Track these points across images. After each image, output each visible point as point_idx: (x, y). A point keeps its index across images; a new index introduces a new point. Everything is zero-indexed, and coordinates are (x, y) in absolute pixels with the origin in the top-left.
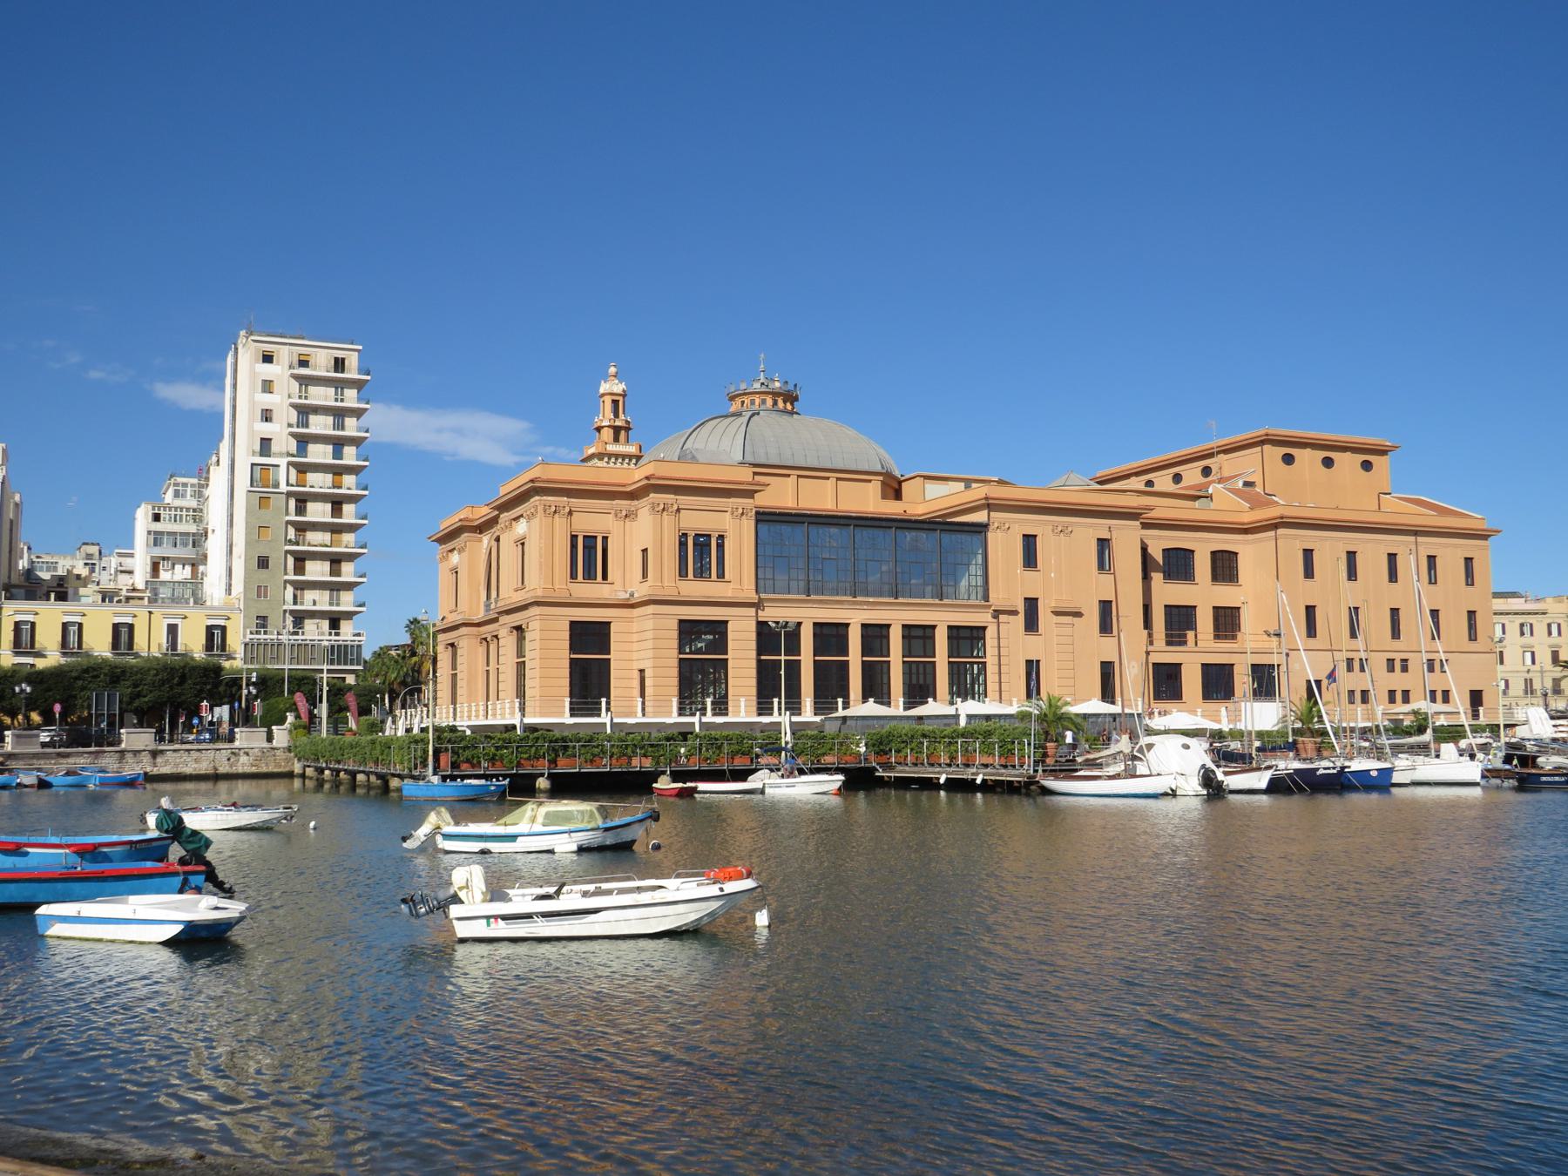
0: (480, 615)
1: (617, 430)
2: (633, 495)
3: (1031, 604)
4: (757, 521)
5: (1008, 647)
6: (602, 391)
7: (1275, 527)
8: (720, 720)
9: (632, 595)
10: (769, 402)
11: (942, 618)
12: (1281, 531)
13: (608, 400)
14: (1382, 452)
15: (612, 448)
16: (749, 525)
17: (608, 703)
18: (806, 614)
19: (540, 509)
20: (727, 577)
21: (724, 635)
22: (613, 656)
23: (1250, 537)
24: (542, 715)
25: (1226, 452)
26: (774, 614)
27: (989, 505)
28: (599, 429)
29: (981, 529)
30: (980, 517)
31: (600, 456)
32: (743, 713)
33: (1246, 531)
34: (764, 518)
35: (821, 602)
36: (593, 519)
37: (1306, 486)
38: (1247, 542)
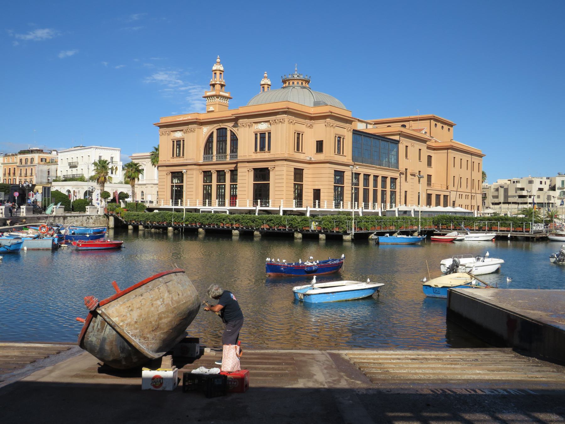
0: (201, 161)
1: (222, 86)
2: (312, 118)
3: (406, 169)
4: (353, 133)
5: (402, 186)
6: (214, 68)
7: (448, 149)
8: (373, 211)
9: (311, 159)
10: (300, 83)
11: (390, 174)
12: (449, 151)
13: (218, 73)
14: (452, 126)
15: (221, 93)
16: (350, 134)
17: (319, 202)
18: (362, 170)
19: (286, 120)
20: (344, 154)
21: (343, 176)
22: (304, 183)
23: (435, 151)
24: (287, 207)
25: (413, 120)
26: (357, 169)
27: (401, 134)
28: (213, 85)
29: (397, 142)
30: (397, 138)
31: (218, 96)
32: (248, 206)
33: (434, 149)
34: (356, 133)
35: (367, 166)
36: (302, 126)
37: (441, 136)
38: (435, 153)
